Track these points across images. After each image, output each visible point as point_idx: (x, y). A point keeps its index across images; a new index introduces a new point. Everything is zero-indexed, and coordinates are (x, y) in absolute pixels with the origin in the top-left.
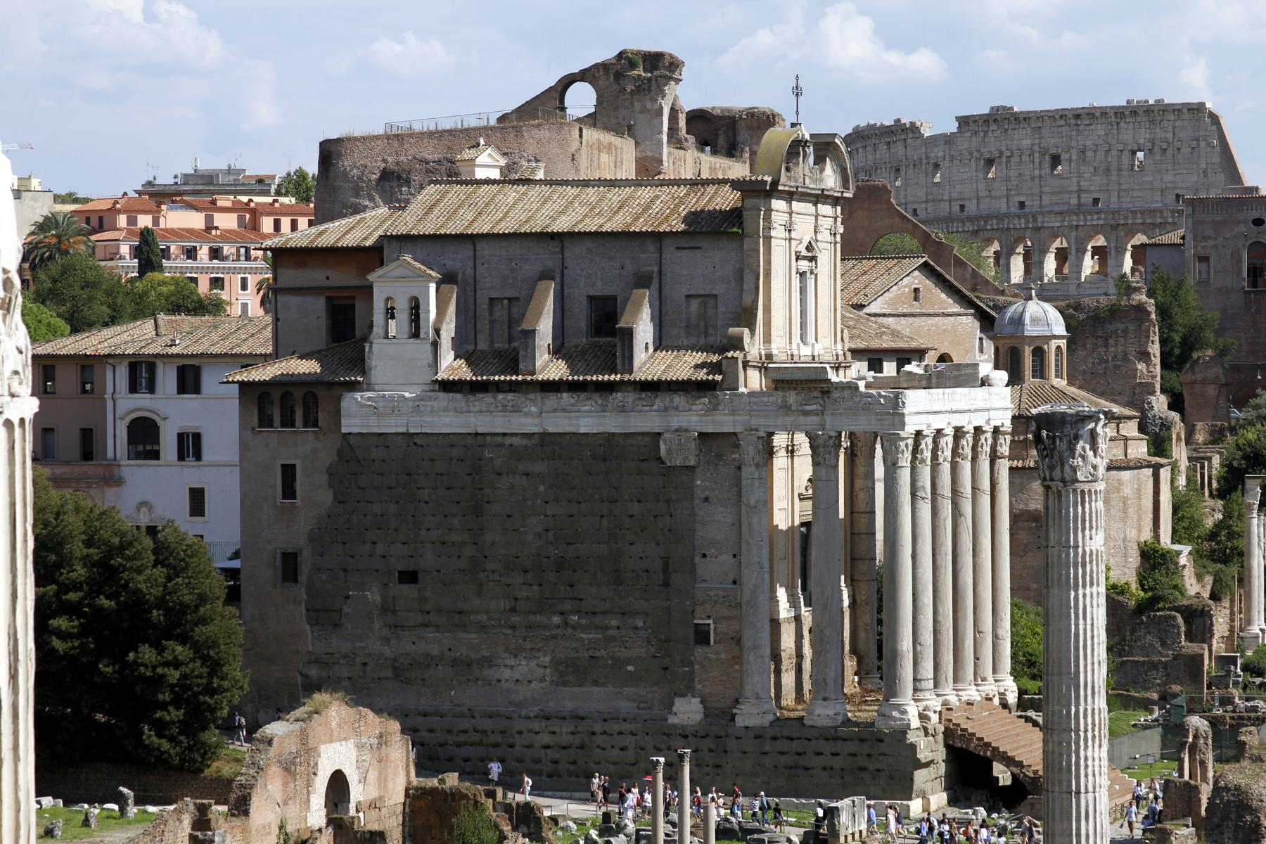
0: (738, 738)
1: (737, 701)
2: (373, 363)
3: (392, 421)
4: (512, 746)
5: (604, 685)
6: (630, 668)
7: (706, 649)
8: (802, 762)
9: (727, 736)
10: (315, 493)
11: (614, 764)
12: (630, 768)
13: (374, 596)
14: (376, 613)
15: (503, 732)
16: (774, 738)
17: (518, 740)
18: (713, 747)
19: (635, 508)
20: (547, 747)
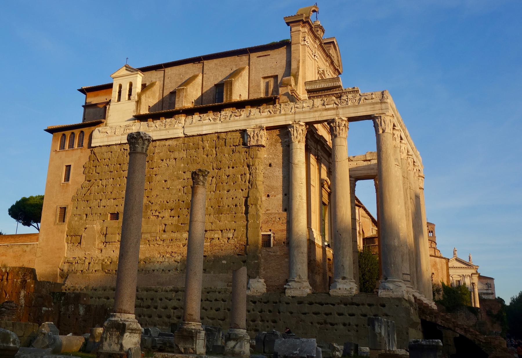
0: (287, 303)
1: (287, 281)
2: (110, 114)
3: (114, 138)
4: (156, 308)
5: (209, 272)
6: (224, 262)
7: (268, 249)
8: (329, 319)
9: (280, 302)
10: (77, 177)
11: (213, 319)
12: (221, 322)
13: (97, 226)
14: (97, 236)
15: (152, 299)
16: (311, 304)
17: (159, 304)
18: (271, 309)
19: (230, 171)
20: (175, 308)
